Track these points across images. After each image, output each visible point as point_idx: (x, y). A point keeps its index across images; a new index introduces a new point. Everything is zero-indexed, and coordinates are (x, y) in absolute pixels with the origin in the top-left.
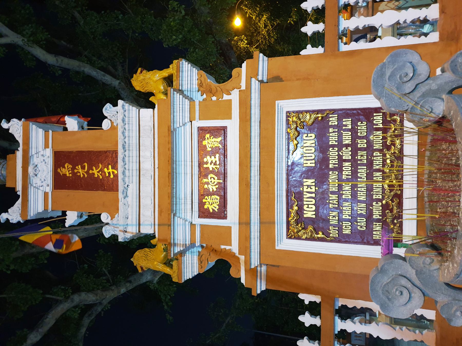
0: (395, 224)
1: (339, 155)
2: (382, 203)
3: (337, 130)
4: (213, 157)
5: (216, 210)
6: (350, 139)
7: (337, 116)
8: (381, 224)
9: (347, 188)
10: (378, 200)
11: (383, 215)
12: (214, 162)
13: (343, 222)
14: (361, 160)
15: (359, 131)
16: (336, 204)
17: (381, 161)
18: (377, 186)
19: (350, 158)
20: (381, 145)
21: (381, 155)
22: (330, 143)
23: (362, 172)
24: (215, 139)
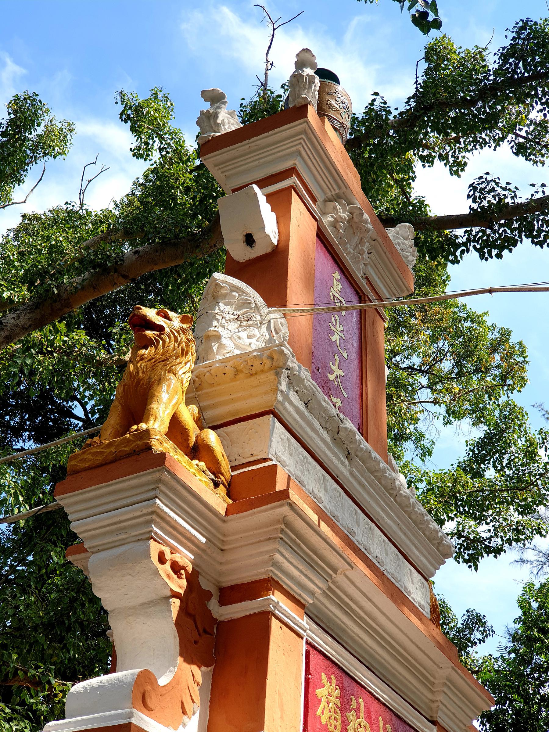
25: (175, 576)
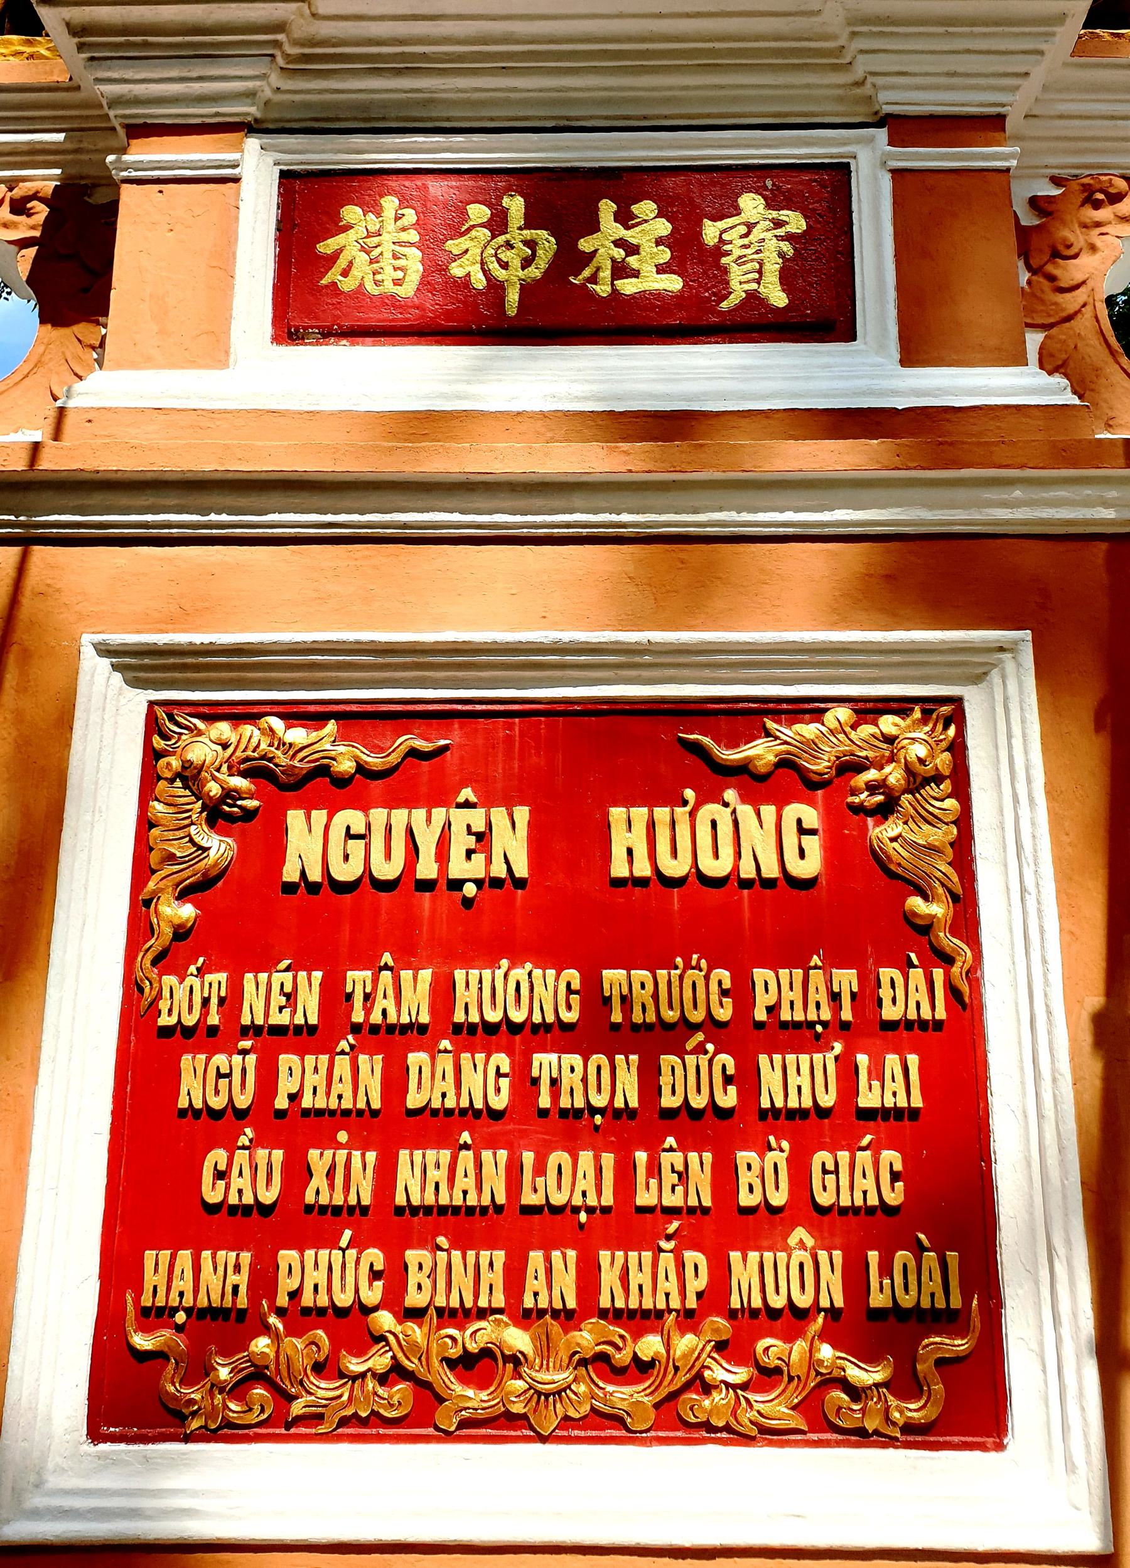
0: (238, 1390)
1: (687, 1027)
2: (375, 1309)
3: (847, 1015)
4: (665, 255)
5: (333, 275)
6: (793, 1103)
7: (941, 1014)
8: (243, 1302)
9: (473, 1081)
10: (394, 1277)
11: (301, 1317)
12: (633, 261)
13: (252, 1059)
14: (654, 1169)
15: (844, 1156)
16: (368, 1011)
17: (648, 1304)
18: (486, 1276)
19: (669, 1101)
20: (757, 1303)
21: (692, 1303)
22: (761, 975)
23: (577, 1179)
24: (773, 267)
25: (23, 218)
